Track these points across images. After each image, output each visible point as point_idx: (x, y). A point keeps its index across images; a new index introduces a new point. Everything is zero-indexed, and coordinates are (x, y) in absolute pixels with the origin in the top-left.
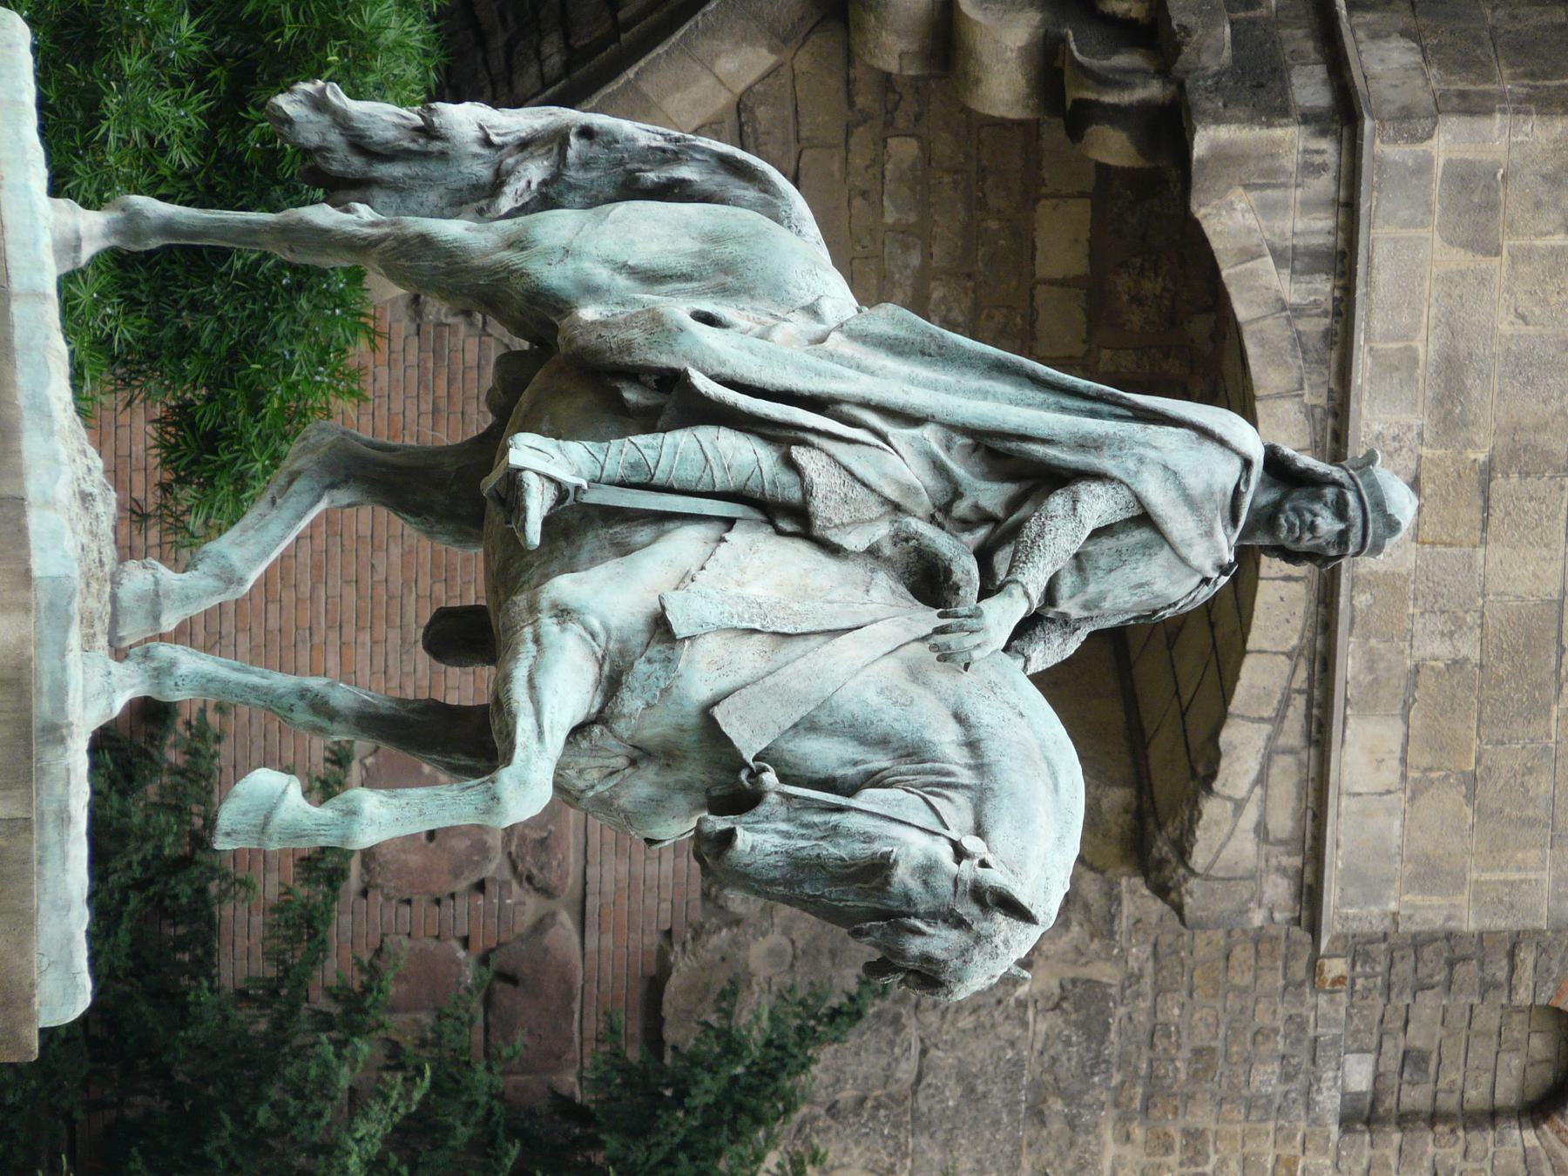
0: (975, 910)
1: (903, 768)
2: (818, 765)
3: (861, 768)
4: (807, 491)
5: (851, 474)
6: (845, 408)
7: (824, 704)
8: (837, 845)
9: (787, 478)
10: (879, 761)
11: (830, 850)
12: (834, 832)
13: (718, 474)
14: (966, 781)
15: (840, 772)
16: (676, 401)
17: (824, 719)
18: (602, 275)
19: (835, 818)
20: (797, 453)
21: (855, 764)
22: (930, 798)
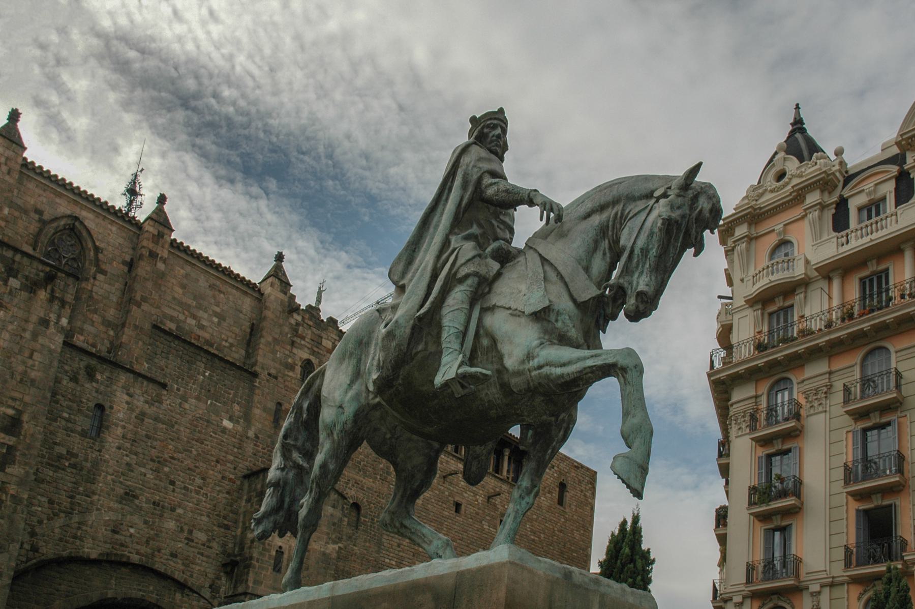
0: (690, 192)
1: (610, 233)
2: (603, 268)
3: (607, 251)
4: (476, 274)
5: (469, 260)
6: (439, 265)
7: (579, 261)
8: (652, 249)
9: (469, 281)
10: (605, 244)
11: (653, 252)
12: (645, 251)
13: (464, 306)
14: (621, 206)
15: (608, 260)
16: (427, 324)
17: (584, 263)
18: (351, 393)
19: (637, 251)
20: (459, 276)
21: (604, 254)
22: (630, 216)
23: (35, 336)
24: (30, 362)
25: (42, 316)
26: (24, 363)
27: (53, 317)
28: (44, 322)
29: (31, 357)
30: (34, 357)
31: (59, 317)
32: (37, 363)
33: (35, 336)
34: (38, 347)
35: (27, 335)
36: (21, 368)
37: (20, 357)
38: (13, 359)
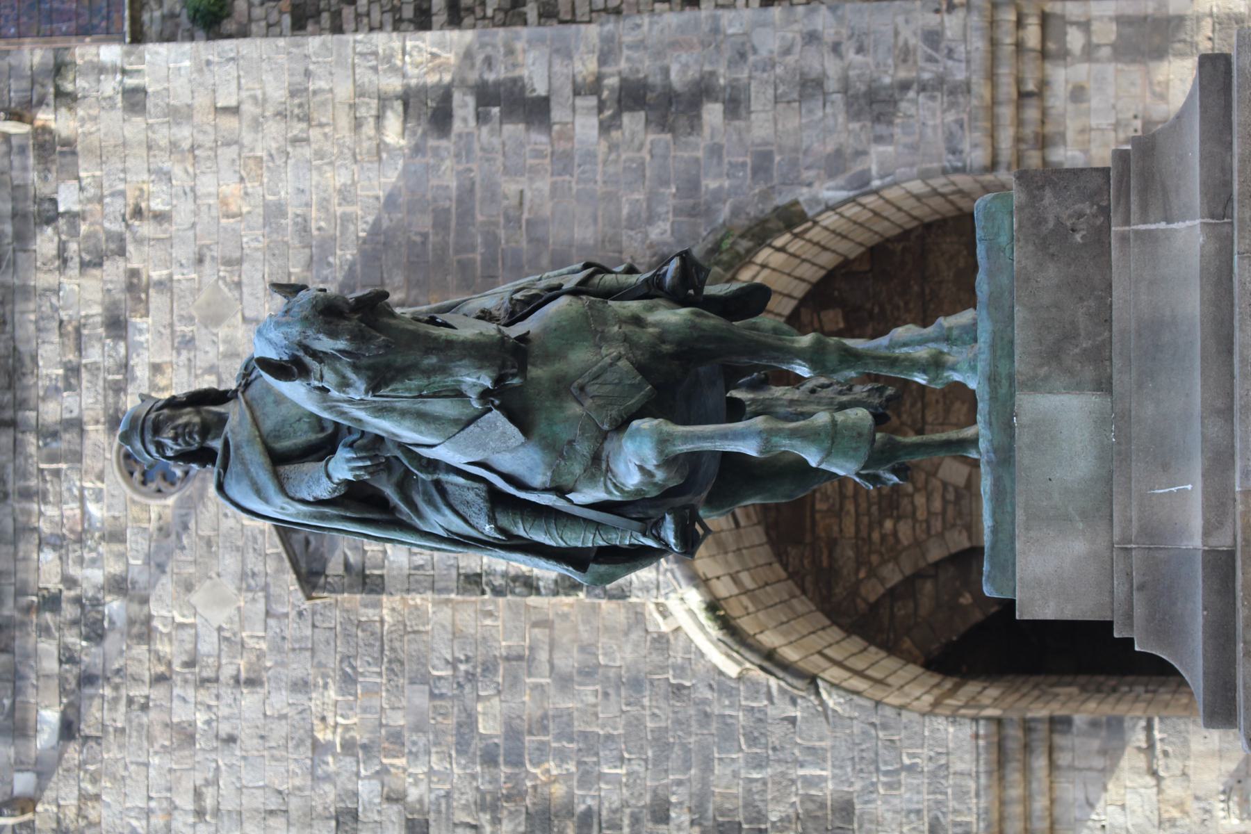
23: (177, 115)
24: (248, 108)
25: (118, 114)
26: (256, 124)
27: (110, 85)
28: (135, 99)
29: (235, 111)
30: (233, 102)
31: (101, 69)
32: (244, 94)
33: (177, 115)
34: (202, 100)
35: (184, 134)
36: (273, 128)
37: (247, 138)
38: (259, 154)
